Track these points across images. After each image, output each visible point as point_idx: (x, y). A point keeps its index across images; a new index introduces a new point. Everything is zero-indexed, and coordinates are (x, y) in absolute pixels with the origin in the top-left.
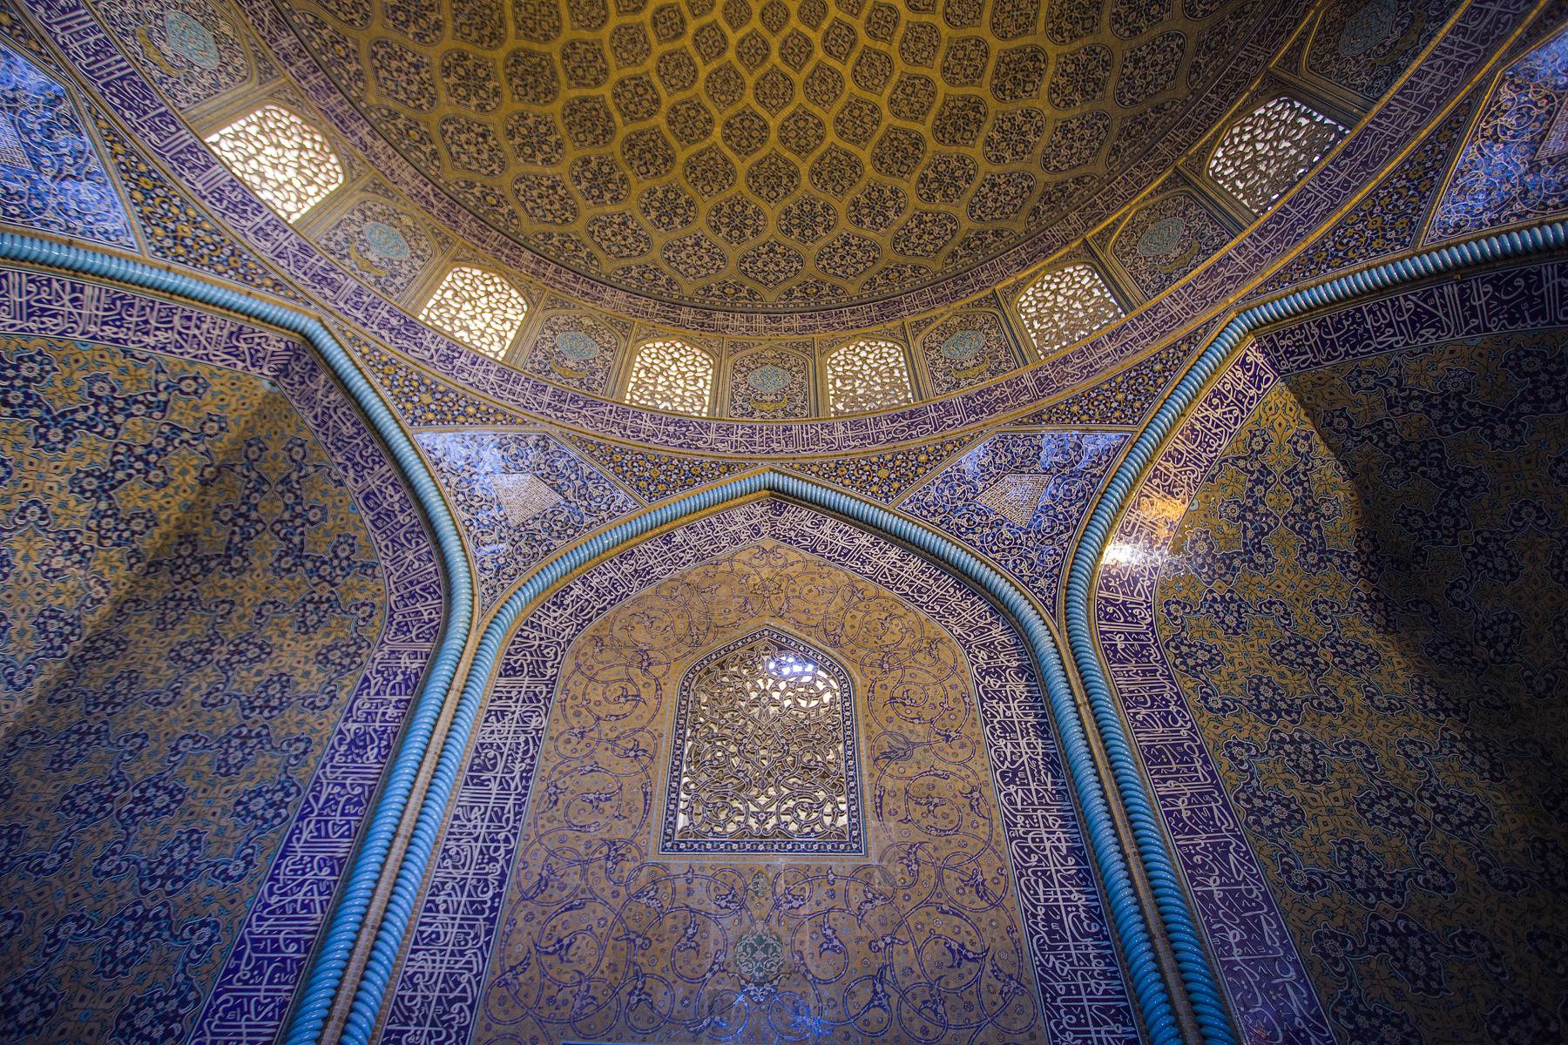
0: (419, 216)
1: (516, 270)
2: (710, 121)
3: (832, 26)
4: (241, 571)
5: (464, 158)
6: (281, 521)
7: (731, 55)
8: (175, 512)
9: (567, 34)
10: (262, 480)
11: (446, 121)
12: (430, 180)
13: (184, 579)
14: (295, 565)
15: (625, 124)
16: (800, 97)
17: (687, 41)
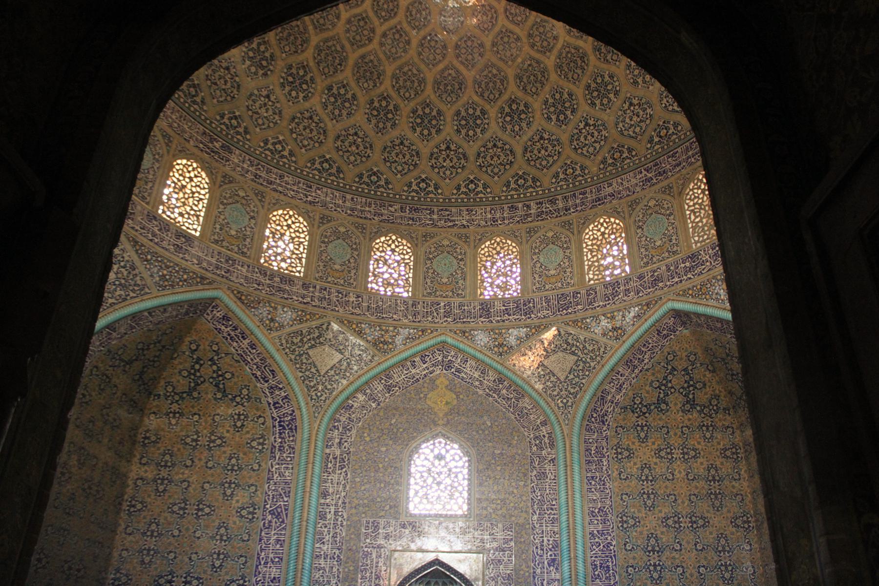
5: (638, 130)
11: (617, 125)
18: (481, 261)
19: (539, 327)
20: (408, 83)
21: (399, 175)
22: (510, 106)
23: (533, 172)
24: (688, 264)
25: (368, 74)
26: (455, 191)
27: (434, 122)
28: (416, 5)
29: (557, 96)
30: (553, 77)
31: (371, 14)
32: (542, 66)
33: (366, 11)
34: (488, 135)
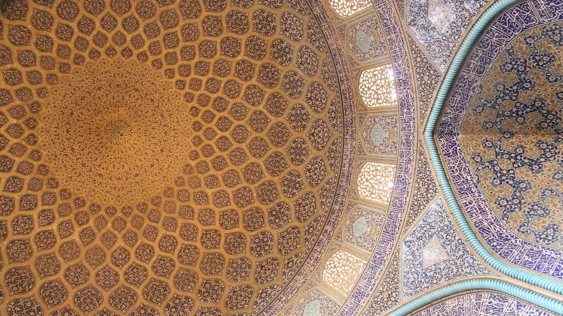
0: (360, 133)
1: (352, 86)
2: (238, 63)
3: (169, 48)
4: (541, 100)
5: (326, 135)
6: (511, 98)
7: (210, 75)
8: (531, 138)
9: (255, 134)
10: (498, 115)
11: (319, 150)
12: (344, 139)
13: (558, 118)
14: (526, 82)
15: (266, 92)
16: (202, 38)
17: (220, 94)
18: (329, 282)
19: (396, 257)
20: (213, 265)
21: (246, 306)
22: (272, 215)
23: (312, 219)
24: (405, 111)
25: (186, 281)
26: (284, 277)
27: (243, 266)
28: (184, 229)
29: (286, 182)
30: (276, 179)
31: (163, 254)
32: (266, 183)
33: (159, 255)
34: (276, 238)
